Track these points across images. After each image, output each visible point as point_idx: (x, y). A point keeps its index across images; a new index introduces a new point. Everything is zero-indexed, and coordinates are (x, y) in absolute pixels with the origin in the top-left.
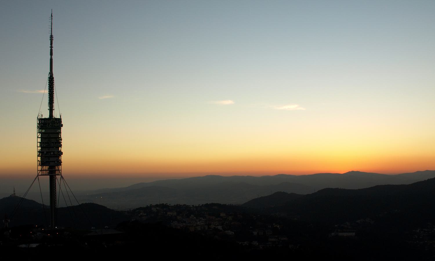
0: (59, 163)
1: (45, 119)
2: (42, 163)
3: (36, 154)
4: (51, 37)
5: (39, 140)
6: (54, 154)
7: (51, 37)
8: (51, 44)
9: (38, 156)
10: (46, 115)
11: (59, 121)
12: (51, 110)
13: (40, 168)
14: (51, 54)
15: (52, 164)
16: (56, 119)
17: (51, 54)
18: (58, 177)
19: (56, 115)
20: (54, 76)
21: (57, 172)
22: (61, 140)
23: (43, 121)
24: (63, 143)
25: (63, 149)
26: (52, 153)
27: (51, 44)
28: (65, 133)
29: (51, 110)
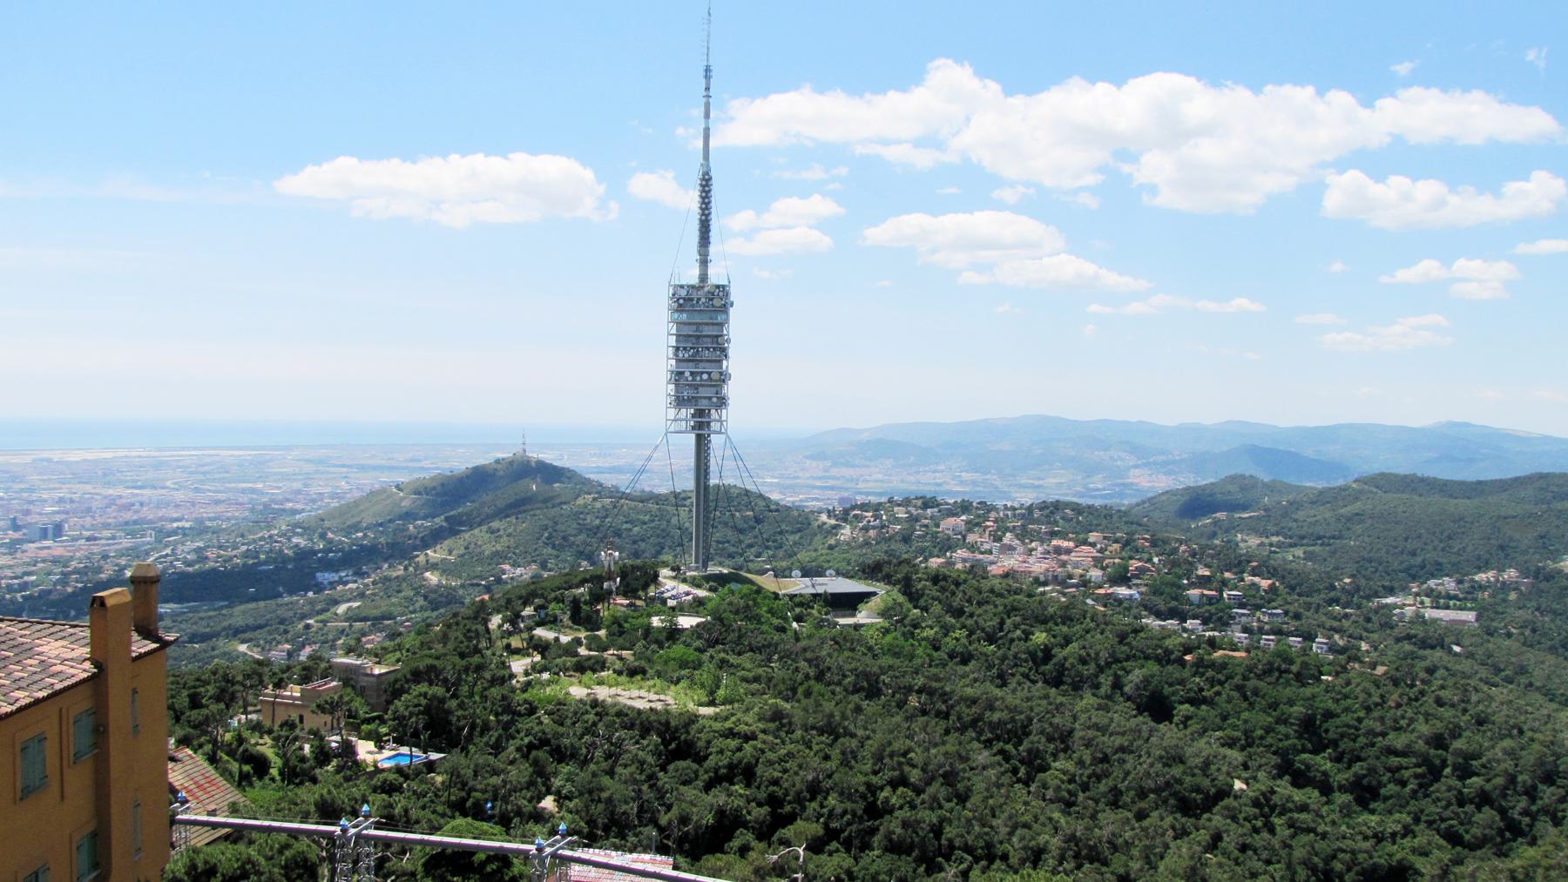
0: (722, 402)
1: (693, 287)
2: (680, 402)
3: (664, 376)
4: (708, 70)
5: (673, 341)
6: (710, 379)
7: (708, 70)
8: (707, 89)
9: (669, 382)
10: (691, 276)
11: (723, 291)
12: (704, 262)
13: (672, 413)
14: (707, 116)
15: (703, 404)
16: (718, 287)
17: (707, 116)
18: (716, 441)
19: (716, 276)
20: (712, 174)
21: (715, 426)
22: (728, 341)
23: (683, 293)
24: (732, 351)
25: (732, 365)
26: (705, 376)
27: (707, 89)
28: (739, 329)
29: (704, 262)
